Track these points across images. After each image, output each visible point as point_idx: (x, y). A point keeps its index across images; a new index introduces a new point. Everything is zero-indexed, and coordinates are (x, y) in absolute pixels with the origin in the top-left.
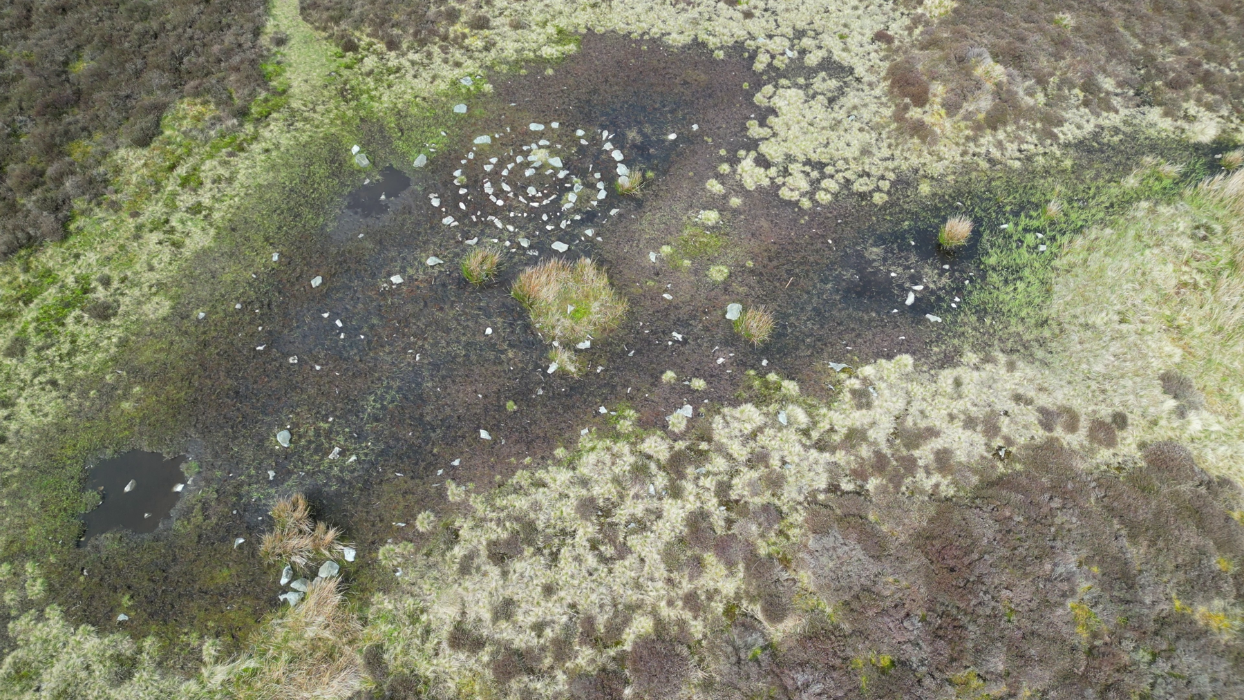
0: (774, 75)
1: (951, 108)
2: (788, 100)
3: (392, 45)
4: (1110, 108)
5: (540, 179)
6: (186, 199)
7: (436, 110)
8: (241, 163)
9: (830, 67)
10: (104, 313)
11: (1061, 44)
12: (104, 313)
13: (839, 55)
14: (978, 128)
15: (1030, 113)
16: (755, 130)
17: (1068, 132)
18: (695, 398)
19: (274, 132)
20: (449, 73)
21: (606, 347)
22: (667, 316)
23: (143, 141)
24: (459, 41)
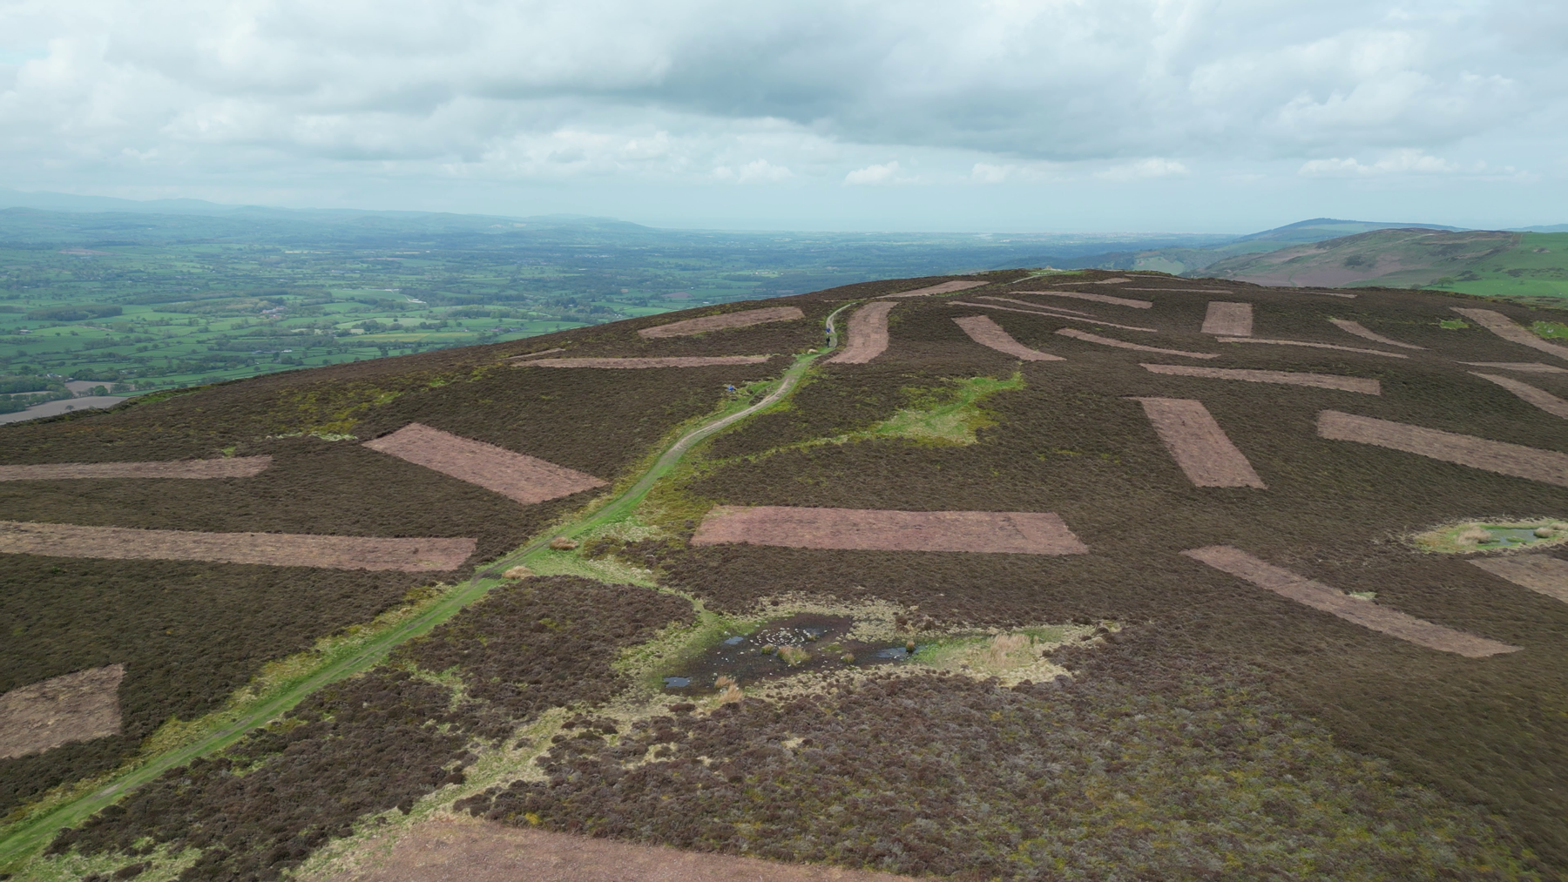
0: (860, 621)
1: (914, 625)
2: (863, 625)
3: (734, 614)
4: (965, 627)
5: (784, 637)
6: (677, 640)
7: (751, 626)
8: (692, 635)
9: (878, 619)
10: (660, 657)
11: (953, 615)
12: (660, 657)
13: (880, 617)
14: (922, 630)
15: (939, 627)
16: (852, 629)
17: (951, 631)
18: (830, 670)
19: (699, 629)
20: (753, 620)
21: (804, 662)
22: (823, 658)
23: (663, 628)
24: (756, 614)
